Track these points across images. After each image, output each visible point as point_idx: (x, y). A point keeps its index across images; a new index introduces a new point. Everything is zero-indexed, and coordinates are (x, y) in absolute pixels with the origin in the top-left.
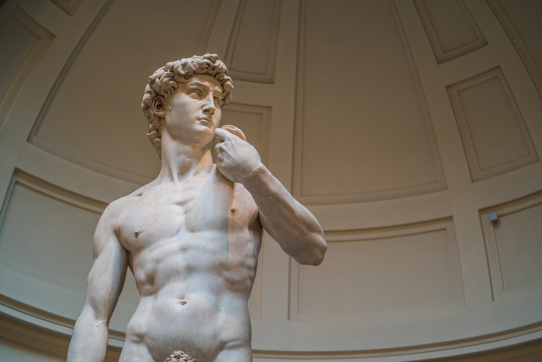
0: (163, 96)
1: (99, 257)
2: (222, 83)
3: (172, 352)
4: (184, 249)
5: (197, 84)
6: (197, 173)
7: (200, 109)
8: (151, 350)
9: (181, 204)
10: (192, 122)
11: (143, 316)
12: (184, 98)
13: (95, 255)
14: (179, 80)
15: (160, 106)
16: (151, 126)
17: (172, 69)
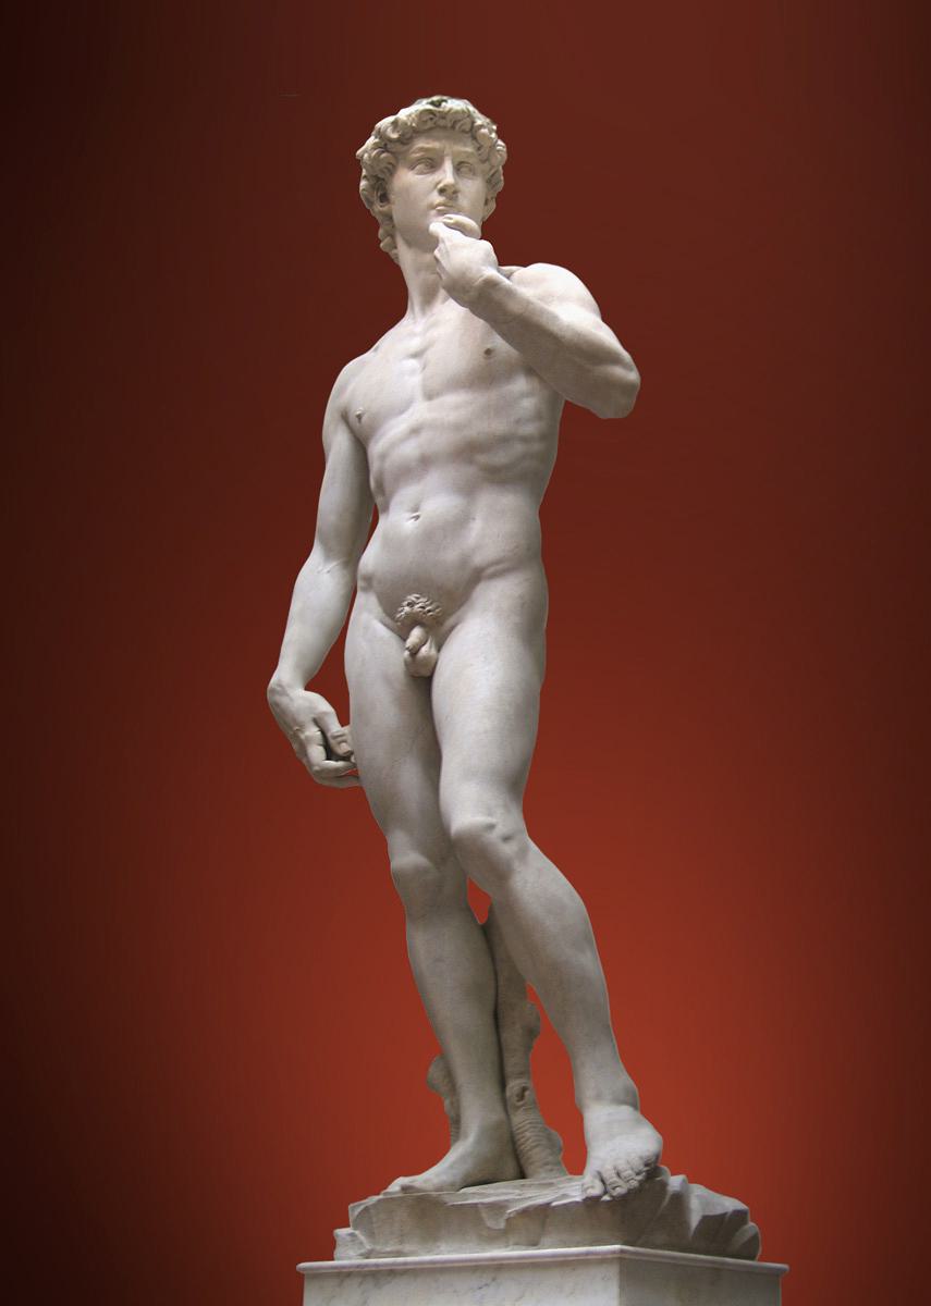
0: (383, 179)
2: (473, 132)
4: (415, 431)
5: (421, 149)
7: (432, 190)
10: (425, 214)
17: (381, 135)
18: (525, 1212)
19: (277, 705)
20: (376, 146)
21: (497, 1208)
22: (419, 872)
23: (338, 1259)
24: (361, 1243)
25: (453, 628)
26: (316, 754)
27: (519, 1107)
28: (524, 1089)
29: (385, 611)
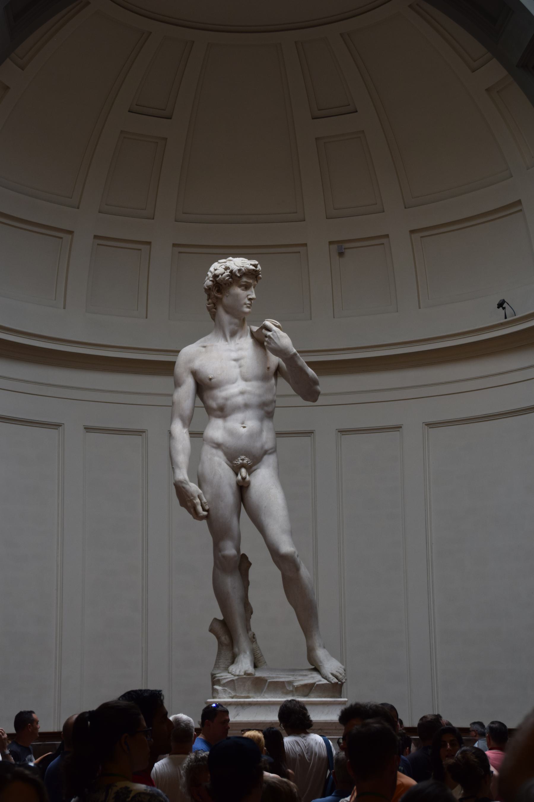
0: (221, 285)
1: (182, 387)
3: (239, 457)
4: (242, 393)
5: (246, 282)
6: (241, 337)
8: (226, 454)
9: (236, 360)
10: (242, 306)
11: (217, 430)
12: (238, 290)
13: (177, 384)
14: (235, 278)
15: (219, 291)
16: (210, 301)
17: (231, 272)
18: (305, 686)
19: (184, 488)
20: (228, 276)
21: (290, 683)
22: (235, 556)
23: (220, 698)
24: (229, 693)
25: (255, 470)
26: (200, 508)
27: (254, 642)
28: (254, 635)
29: (228, 459)
